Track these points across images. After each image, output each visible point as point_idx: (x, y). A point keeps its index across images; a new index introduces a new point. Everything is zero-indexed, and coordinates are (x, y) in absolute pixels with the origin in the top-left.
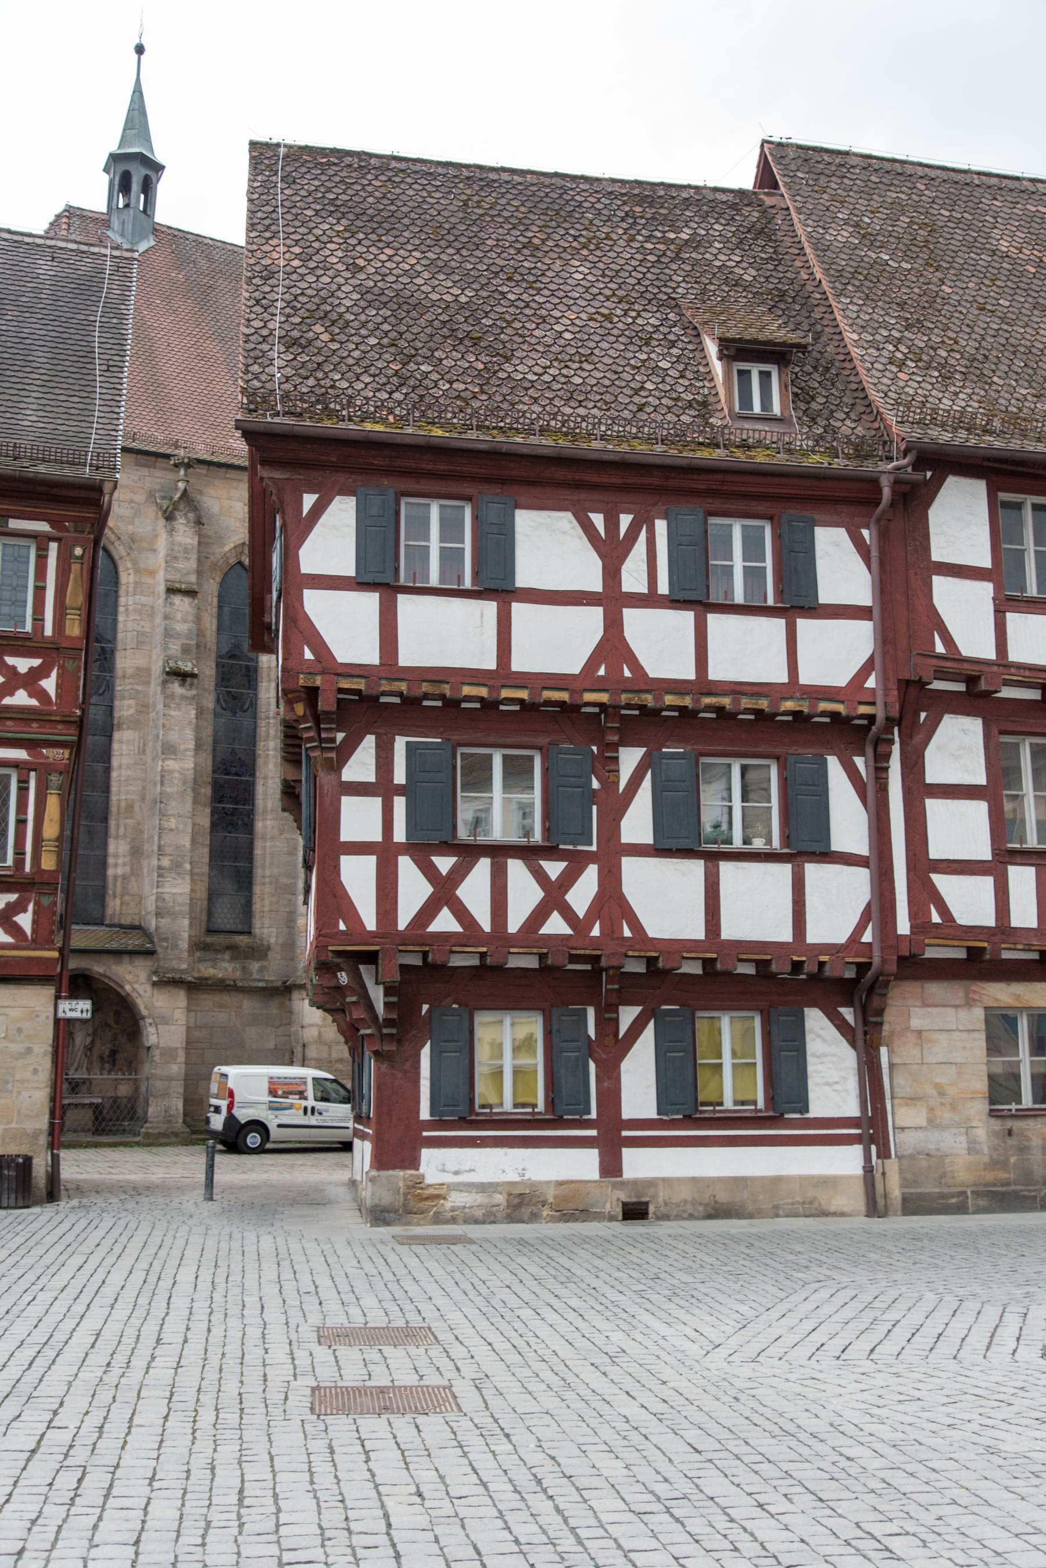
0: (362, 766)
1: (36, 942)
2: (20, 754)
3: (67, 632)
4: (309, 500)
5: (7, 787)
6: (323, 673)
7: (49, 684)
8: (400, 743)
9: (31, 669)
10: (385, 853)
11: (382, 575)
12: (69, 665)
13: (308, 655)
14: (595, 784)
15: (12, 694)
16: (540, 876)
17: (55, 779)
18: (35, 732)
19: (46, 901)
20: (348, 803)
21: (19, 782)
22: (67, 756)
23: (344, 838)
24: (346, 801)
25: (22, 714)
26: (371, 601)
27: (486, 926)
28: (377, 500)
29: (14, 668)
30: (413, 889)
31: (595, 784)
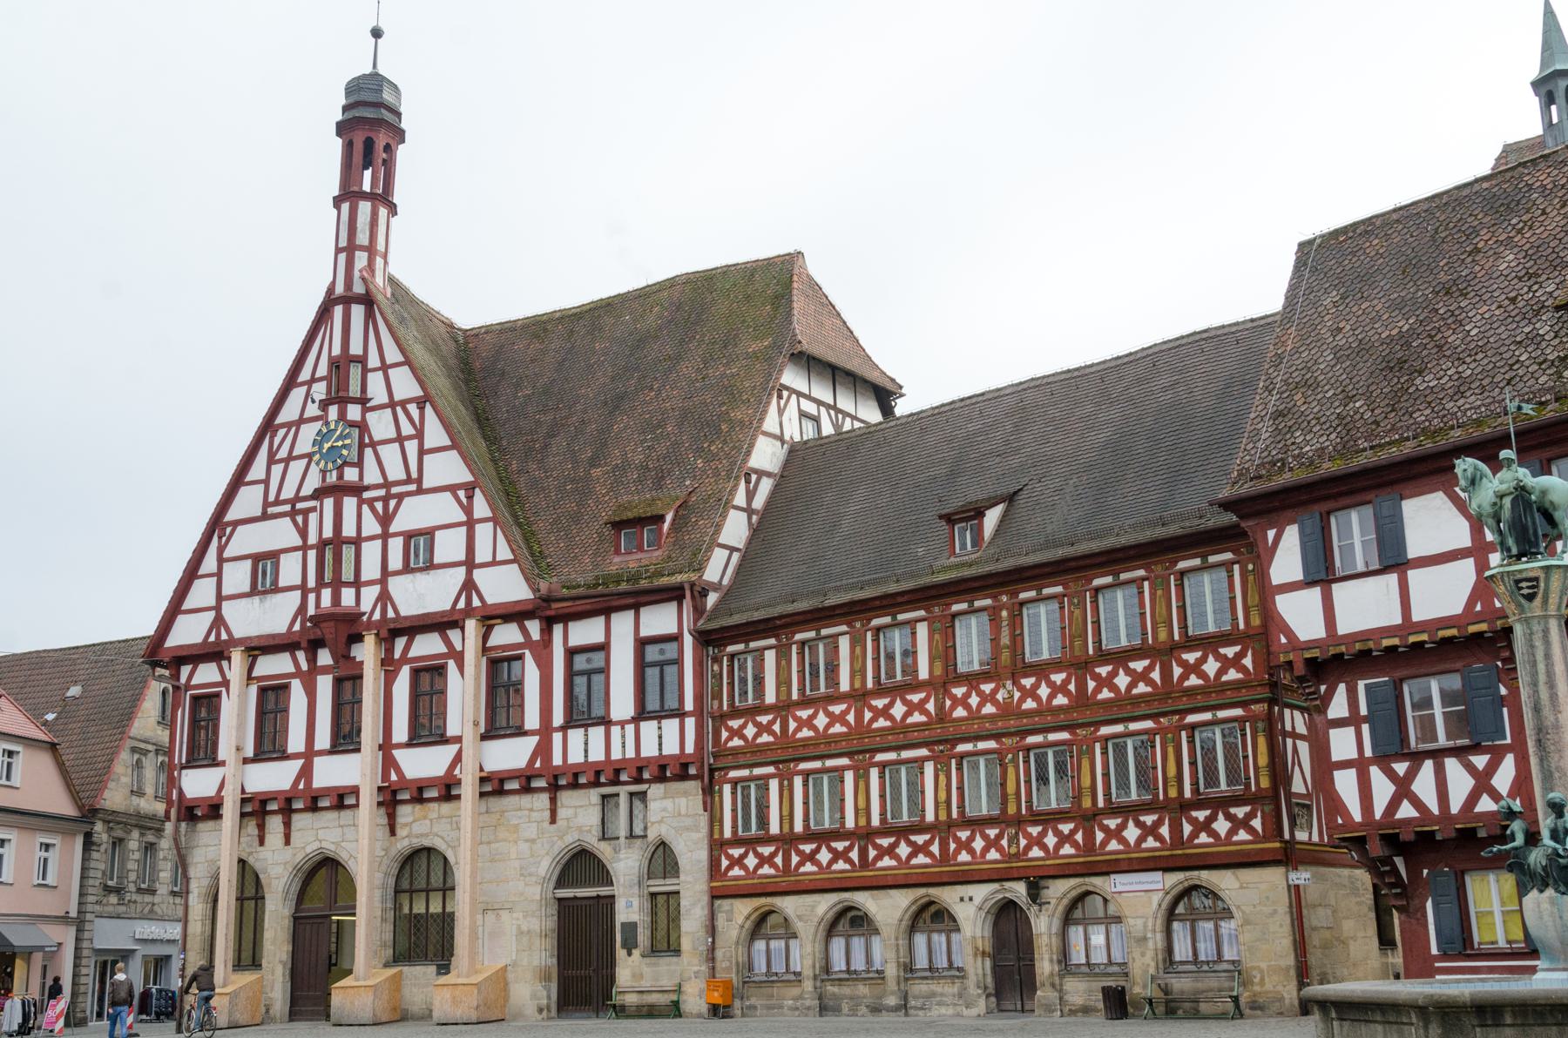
0: (1338, 707)
1: (1265, 839)
4: (1271, 534)
6: (1294, 650)
7: (1248, 662)
8: (1361, 685)
10: (1360, 765)
11: (1322, 572)
13: (1283, 640)
14: (1503, 691)
16: (1471, 768)
18: (1244, 695)
19: (1267, 809)
20: (1334, 734)
23: (1334, 758)
24: (1333, 732)
25: (1235, 685)
26: (1315, 593)
27: (1435, 809)
28: (1308, 523)
30: (1383, 790)
31: (1503, 691)
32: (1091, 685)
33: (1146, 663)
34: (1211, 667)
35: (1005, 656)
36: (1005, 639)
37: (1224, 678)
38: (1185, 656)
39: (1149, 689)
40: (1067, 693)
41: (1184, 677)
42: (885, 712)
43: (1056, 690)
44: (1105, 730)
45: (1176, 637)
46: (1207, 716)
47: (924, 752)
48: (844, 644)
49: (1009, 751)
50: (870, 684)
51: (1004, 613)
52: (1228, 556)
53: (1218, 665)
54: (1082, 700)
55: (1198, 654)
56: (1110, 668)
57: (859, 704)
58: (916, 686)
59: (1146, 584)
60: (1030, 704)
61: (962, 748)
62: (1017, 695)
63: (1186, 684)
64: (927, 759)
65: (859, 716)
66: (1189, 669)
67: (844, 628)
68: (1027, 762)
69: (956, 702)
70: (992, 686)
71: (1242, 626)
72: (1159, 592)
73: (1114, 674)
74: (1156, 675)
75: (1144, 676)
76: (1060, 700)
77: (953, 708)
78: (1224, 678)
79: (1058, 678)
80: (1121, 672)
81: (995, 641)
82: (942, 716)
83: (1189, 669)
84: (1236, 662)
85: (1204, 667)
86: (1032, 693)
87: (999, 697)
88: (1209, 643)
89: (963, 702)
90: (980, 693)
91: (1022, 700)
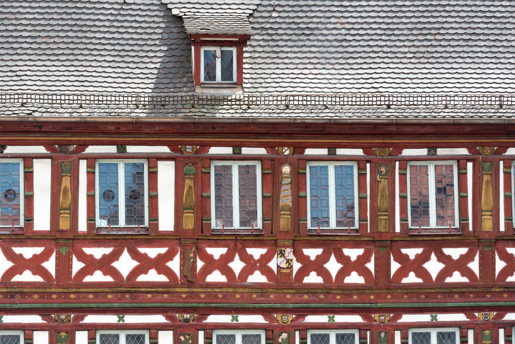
32: (395, 266)
33: (464, 251)
35: (284, 222)
36: (286, 198)
39: (465, 280)
40: (364, 272)
42: (105, 264)
43: (348, 266)
44: (407, 318)
45: (502, 228)
47: (159, 319)
48: (43, 171)
49: (283, 329)
50: (82, 226)
51: (286, 169)
54: (382, 282)
56: (420, 251)
57: (64, 251)
58: (154, 237)
59: (470, 165)
60: (313, 278)
61: (213, 319)
62: (297, 266)
64: (163, 327)
65: (63, 265)
67: (41, 150)
69: (211, 264)
70: (264, 251)
72: (486, 178)
73: (424, 258)
74: (474, 266)
76: (354, 278)
77: (207, 271)
79: (353, 253)
80: (433, 256)
81: (271, 201)
82: (191, 278)
86: (318, 266)
87: (273, 265)
89: (223, 265)
90: (246, 258)
91: (304, 272)
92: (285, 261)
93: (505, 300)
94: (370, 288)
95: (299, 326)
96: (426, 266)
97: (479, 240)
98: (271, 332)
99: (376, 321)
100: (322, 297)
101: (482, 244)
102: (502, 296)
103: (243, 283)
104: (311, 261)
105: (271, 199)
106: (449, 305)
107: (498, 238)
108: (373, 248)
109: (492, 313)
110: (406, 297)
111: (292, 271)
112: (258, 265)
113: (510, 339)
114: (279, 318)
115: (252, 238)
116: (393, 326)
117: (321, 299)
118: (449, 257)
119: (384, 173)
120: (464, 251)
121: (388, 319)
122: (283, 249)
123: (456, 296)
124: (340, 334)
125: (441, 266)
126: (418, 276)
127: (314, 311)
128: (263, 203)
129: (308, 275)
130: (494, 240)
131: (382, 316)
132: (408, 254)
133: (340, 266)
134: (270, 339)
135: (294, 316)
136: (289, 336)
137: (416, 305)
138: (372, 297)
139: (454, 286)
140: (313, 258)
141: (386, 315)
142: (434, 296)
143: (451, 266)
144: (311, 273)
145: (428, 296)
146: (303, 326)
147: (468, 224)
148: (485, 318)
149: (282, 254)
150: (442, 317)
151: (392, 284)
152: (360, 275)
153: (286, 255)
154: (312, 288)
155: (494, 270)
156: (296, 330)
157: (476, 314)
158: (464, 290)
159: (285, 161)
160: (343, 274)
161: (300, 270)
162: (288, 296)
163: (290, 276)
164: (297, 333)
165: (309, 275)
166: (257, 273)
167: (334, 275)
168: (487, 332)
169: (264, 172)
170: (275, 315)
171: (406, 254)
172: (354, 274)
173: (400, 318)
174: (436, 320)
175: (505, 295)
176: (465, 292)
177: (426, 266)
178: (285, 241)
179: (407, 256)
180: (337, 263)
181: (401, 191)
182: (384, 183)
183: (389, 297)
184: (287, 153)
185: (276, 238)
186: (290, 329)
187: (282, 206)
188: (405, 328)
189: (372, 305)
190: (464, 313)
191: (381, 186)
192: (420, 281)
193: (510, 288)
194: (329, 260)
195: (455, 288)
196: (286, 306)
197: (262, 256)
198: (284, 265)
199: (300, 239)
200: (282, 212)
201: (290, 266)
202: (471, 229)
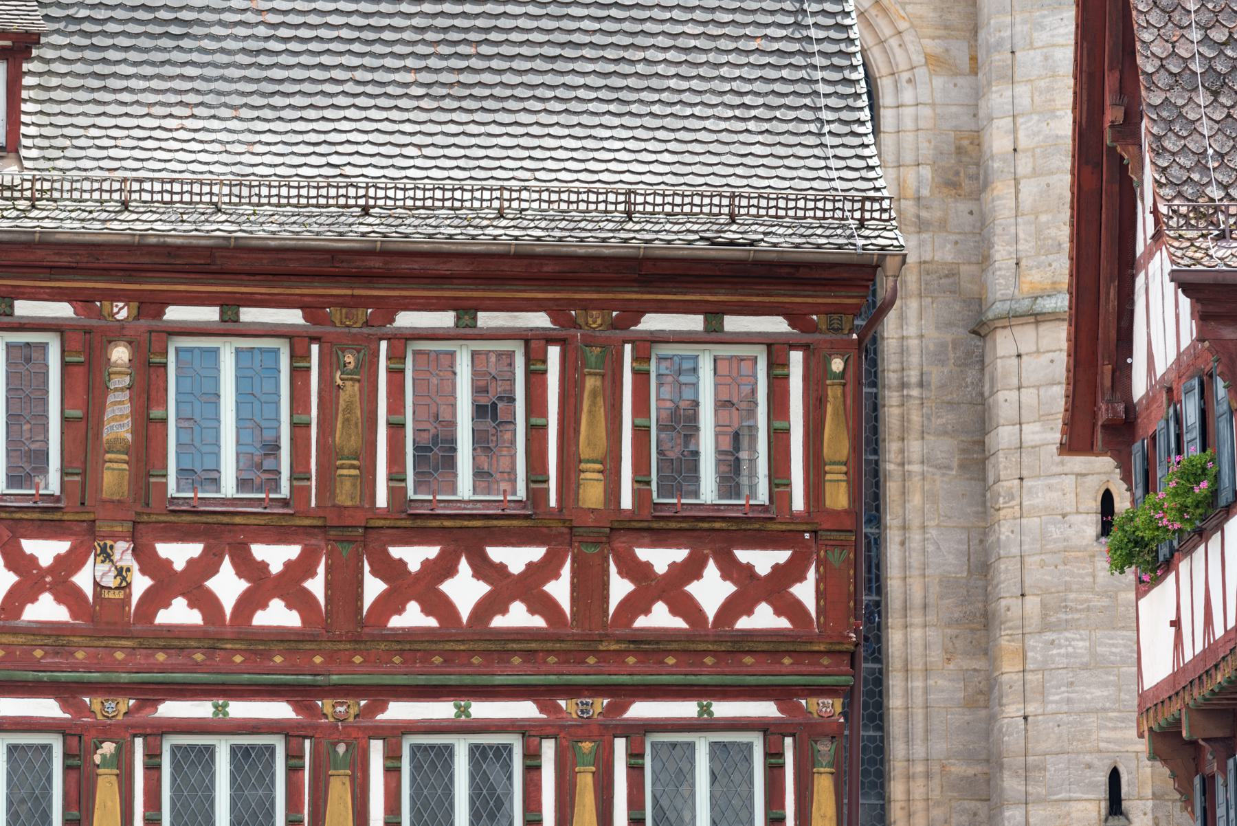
2: (766, 709)
3: (829, 503)
5: (749, 759)
7: (805, 592)
9: (776, 568)
12: (836, 557)
15: (749, 612)
17: (825, 748)
18: (787, 670)
21: (767, 755)
22: (839, 709)
29: (749, 568)
32: (373, 588)
33: (536, 553)
34: (711, 591)
35: (114, 478)
36: (118, 422)
37: (743, 623)
38: (643, 554)
39: (538, 622)
40: (300, 600)
41: (636, 605)
44: (399, 711)
45: (627, 502)
46: (687, 709)
49: (106, 731)
51: (120, 354)
52: (777, 325)
53: (729, 588)
54: (342, 625)
55: (680, 555)
56: (432, 552)
59: (554, 353)
60: (179, 613)
62: (141, 584)
63: (641, 622)
66: (650, 587)
68: (153, 767)
70: (63, 547)
71: (798, 504)
72: (590, 383)
73: (443, 568)
74: (560, 589)
75: (528, 587)
76: (277, 615)
78: (743, 623)
79: (275, 556)
80: (464, 566)
81: (83, 429)
83: (650, 587)
84: (775, 588)
85: (693, 588)
86: (192, 585)
87: (84, 580)
88: (715, 535)
91: (156, 599)
92: (114, 572)
93: (630, 671)
94: (313, 639)
95: (144, 726)
96: (447, 587)
97: (571, 528)
98: (77, 739)
99: (325, 716)
100: (199, 657)
101: (579, 539)
102: (624, 662)
103: (13, 623)
104: (176, 572)
105: (82, 425)
106: (499, 680)
107: (616, 525)
108: (322, 544)
109: (600, 700)
110: (397, 659)
111: (130, 594)
112: (48, 579)
113: (640, 761)
114: (97, 707)
115: (35, 516)
116: (366, 728)
117: (197, 664)
118: (502, 568)
119: (351, 366)
120: (536, 553)
121: (354, 711)
122: (109, 543)
123: (517, 660)
124: (240, 747)
125: (483, 588)
126: (427, 611)
127: (181, 690)
128: (62, 433)
129: (167, 605)
130: (608, 530)
131: (341, 704)
132: (405, 559)
133: (243, 585)
134: (74, 756)
135: (132, 702)
136: (119, 750)
137: (422, 680)
138: (318, 660)
139: (512, 637)
140: (179, 566)
141: (350, 702)
142: (463, 660)
143: (504, 588)
144: (174, 602)
145: (449, 657)
146: (152, 726)
147: (547, 490)
148: (582, 711)
149: (107, 556)
150: (482, 710)
151: (367, 630)
152: (289, 606)
153: (116, 557)
154: (177, 637)
155: (605, 599)
156: (135, 736)
157: (562, 703)
158: (534, 646)
159: (117, 333)
160: (250, 603)
161: (148, 595)
162: (119, 655)
163: (124, 608)
164: (139, 742)
165: (170, 604)
166: (46, 599)
167: (228, 605)
168: (587, 746)
169: (67, 359)
170: (87, 700)
171: (401, 560)
172: (277, 604)
173: (383, 709)
174: (469, 715)
175: (631, 660)
176: (536, 651)
177: (447, 587)
178: (114, 523)
179: (402, 564)
180: (236, 578)
181: (391, 410)
182: (351, 391)
183: (358, 659)
184: (123, 314)
185: (92, 517)
186: (122, 733)
187: (108, 441)
188: (394, 734)
189: (319, 678)
190: (534, 701)
191: (343, 397)
192: (432, 622)
193: (642, 642)
194: (217, 571)
195: (514, 641)
196: (113, 677)
197: (58, 559)
198: (110, 581)
199: (149, 519)
200: (108, 456)
201: (124, 584)
202: (553, 503)
